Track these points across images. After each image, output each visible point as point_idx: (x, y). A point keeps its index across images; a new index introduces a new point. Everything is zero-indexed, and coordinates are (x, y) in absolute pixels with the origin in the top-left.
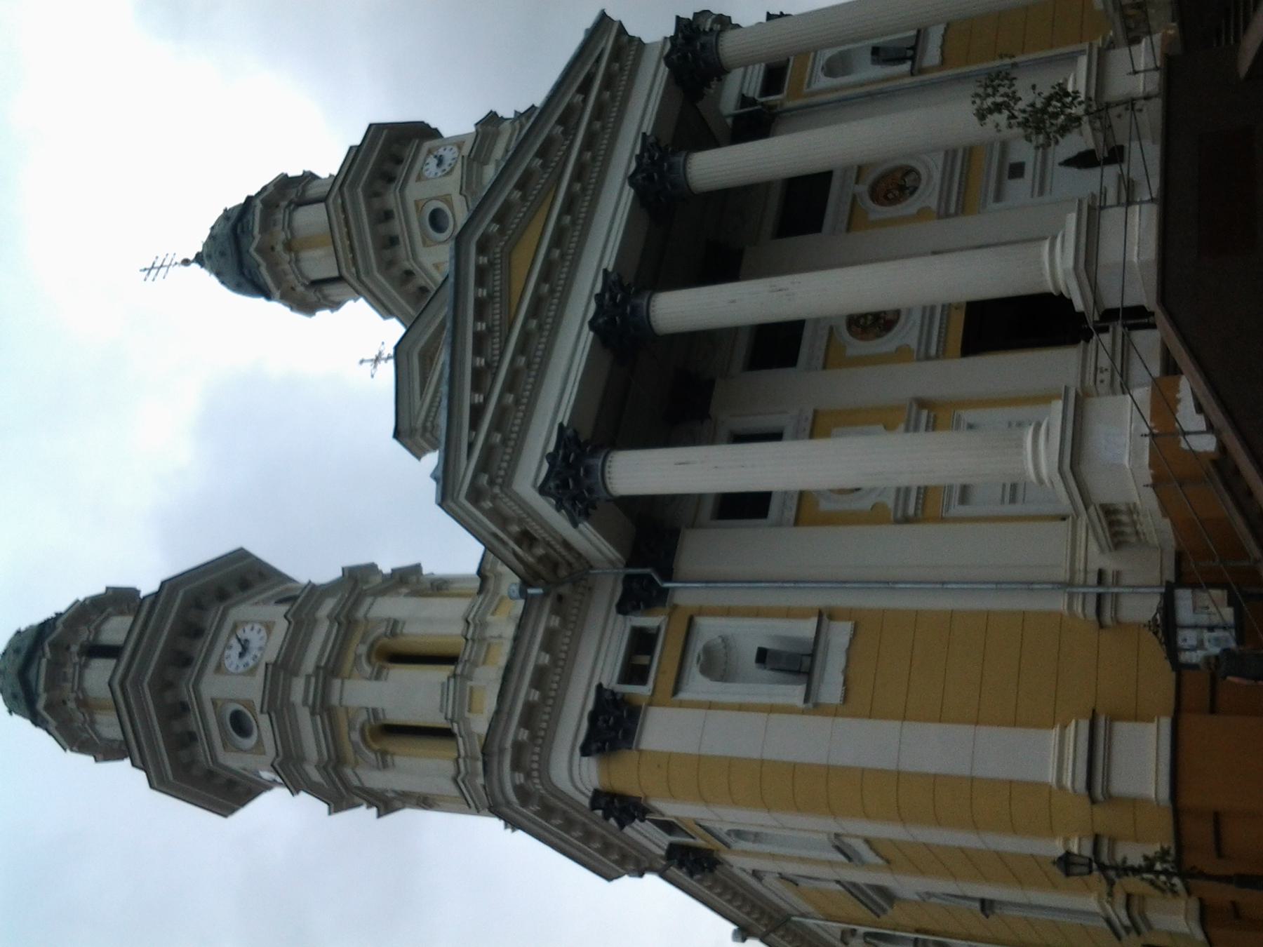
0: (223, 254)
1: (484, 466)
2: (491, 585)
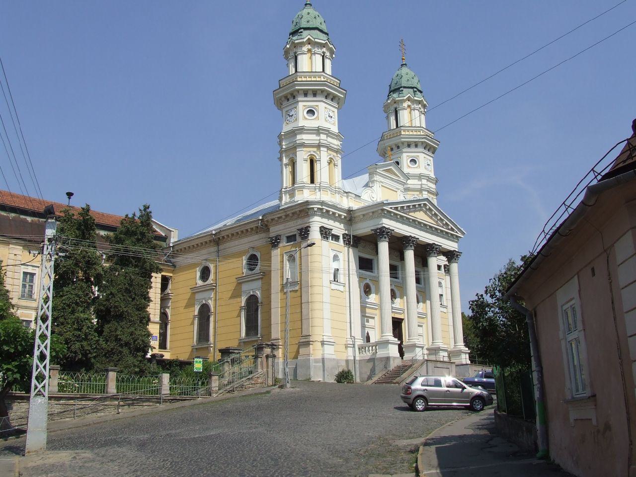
0: (408, 80)
1: (388, 211)
2: (345, 195)
